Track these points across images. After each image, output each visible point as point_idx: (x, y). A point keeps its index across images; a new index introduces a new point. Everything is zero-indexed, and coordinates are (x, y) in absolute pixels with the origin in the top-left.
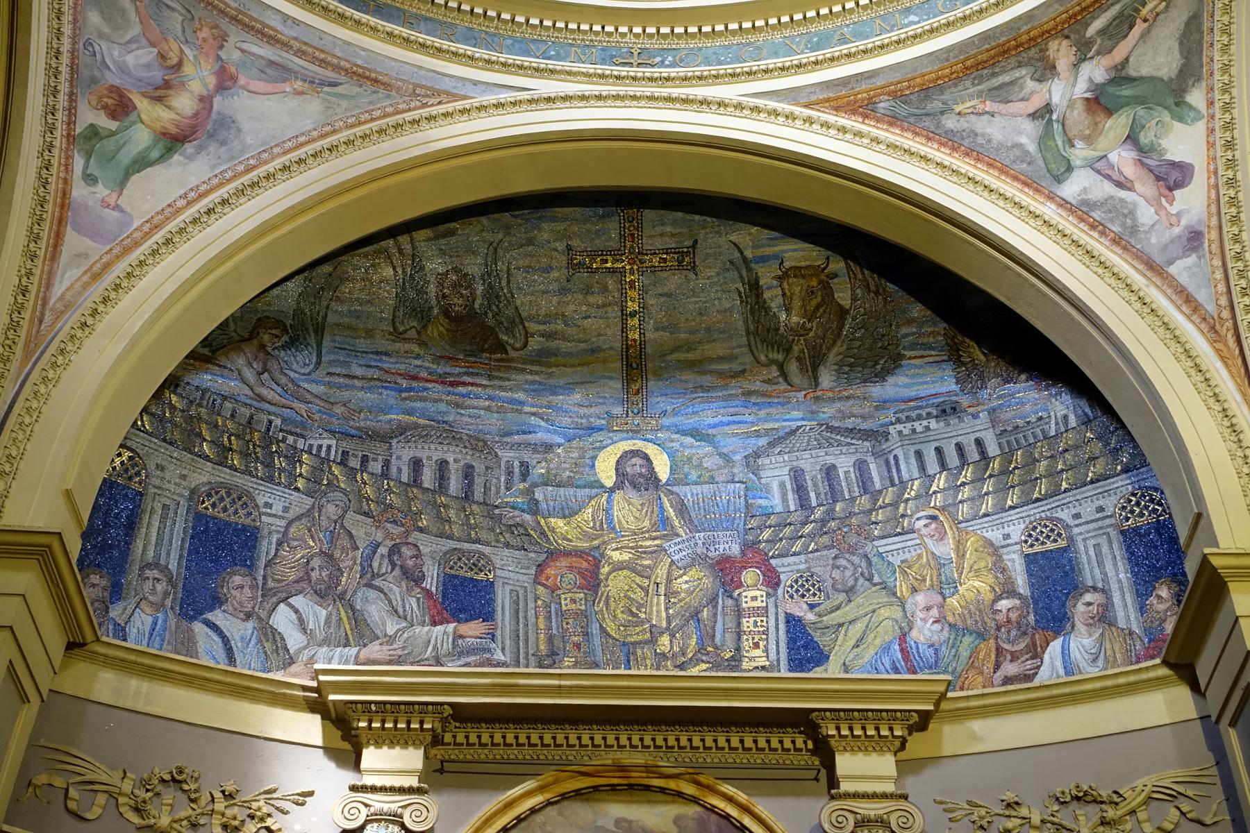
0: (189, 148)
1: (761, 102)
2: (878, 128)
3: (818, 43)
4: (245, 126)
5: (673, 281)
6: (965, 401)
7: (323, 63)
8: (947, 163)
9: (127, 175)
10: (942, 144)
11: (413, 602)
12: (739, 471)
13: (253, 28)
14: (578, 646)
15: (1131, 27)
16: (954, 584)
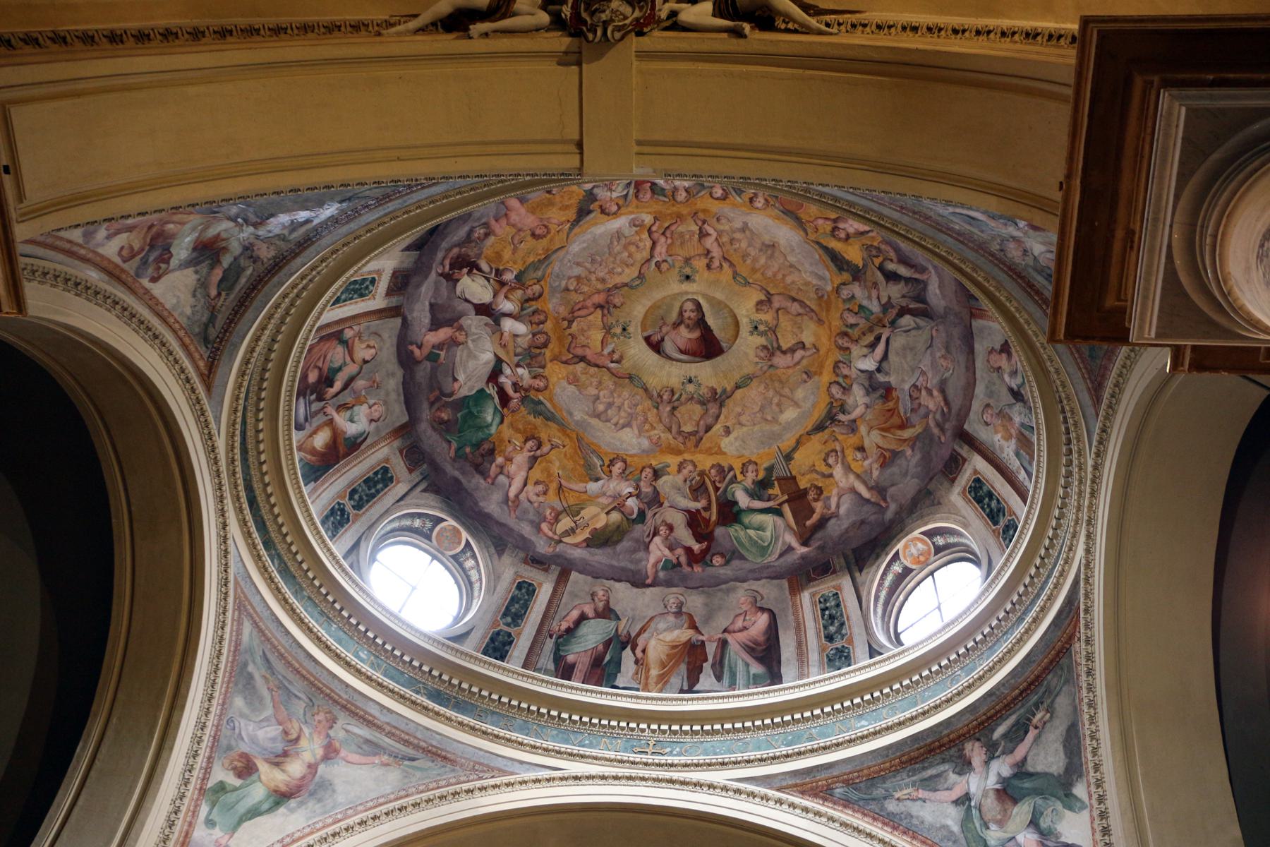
0: (293, 803)
1: (742, 786)
2: (834, 809)
3: (792, 740)
4: (339, 788)
7: (407, 743)
8: (887, 840)
9: (241, 821)
10: (885, 824)
13: (357, 714)
15: (1026, 732)
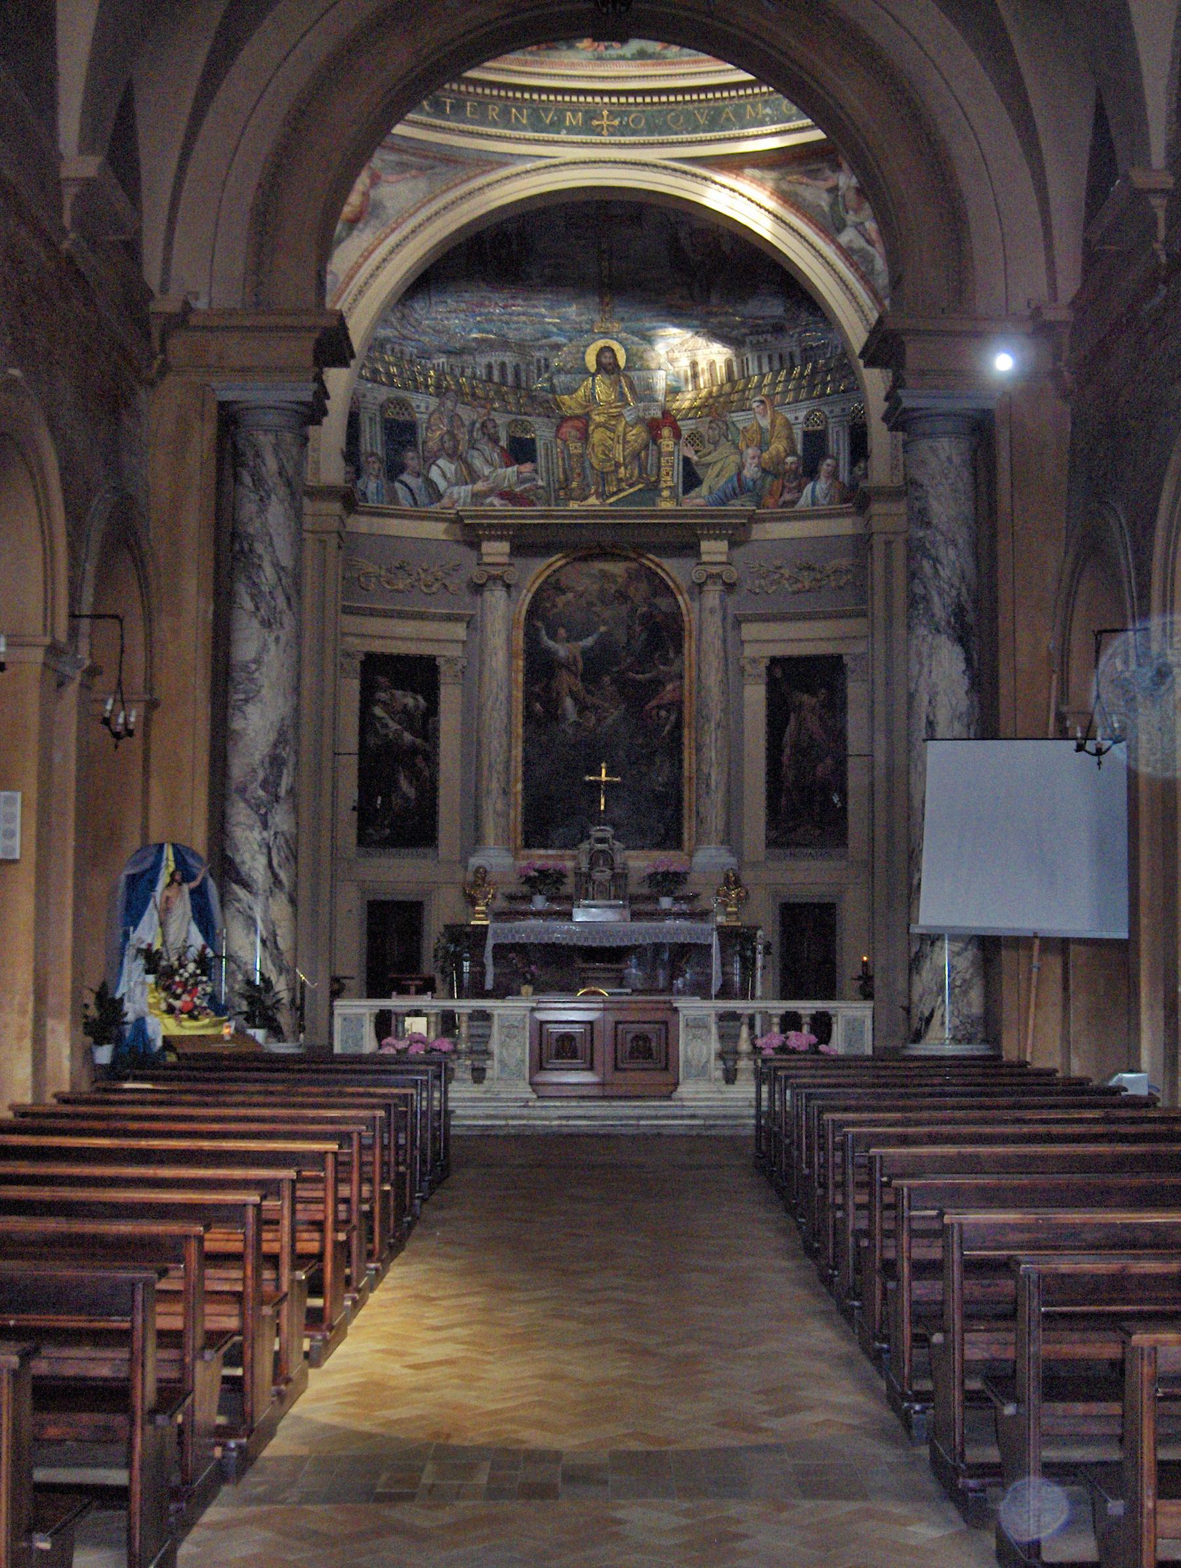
0: (360, 225)
4: (388, 204)
11: (496, 455)
14: (579, 475)
16: (768, 445)
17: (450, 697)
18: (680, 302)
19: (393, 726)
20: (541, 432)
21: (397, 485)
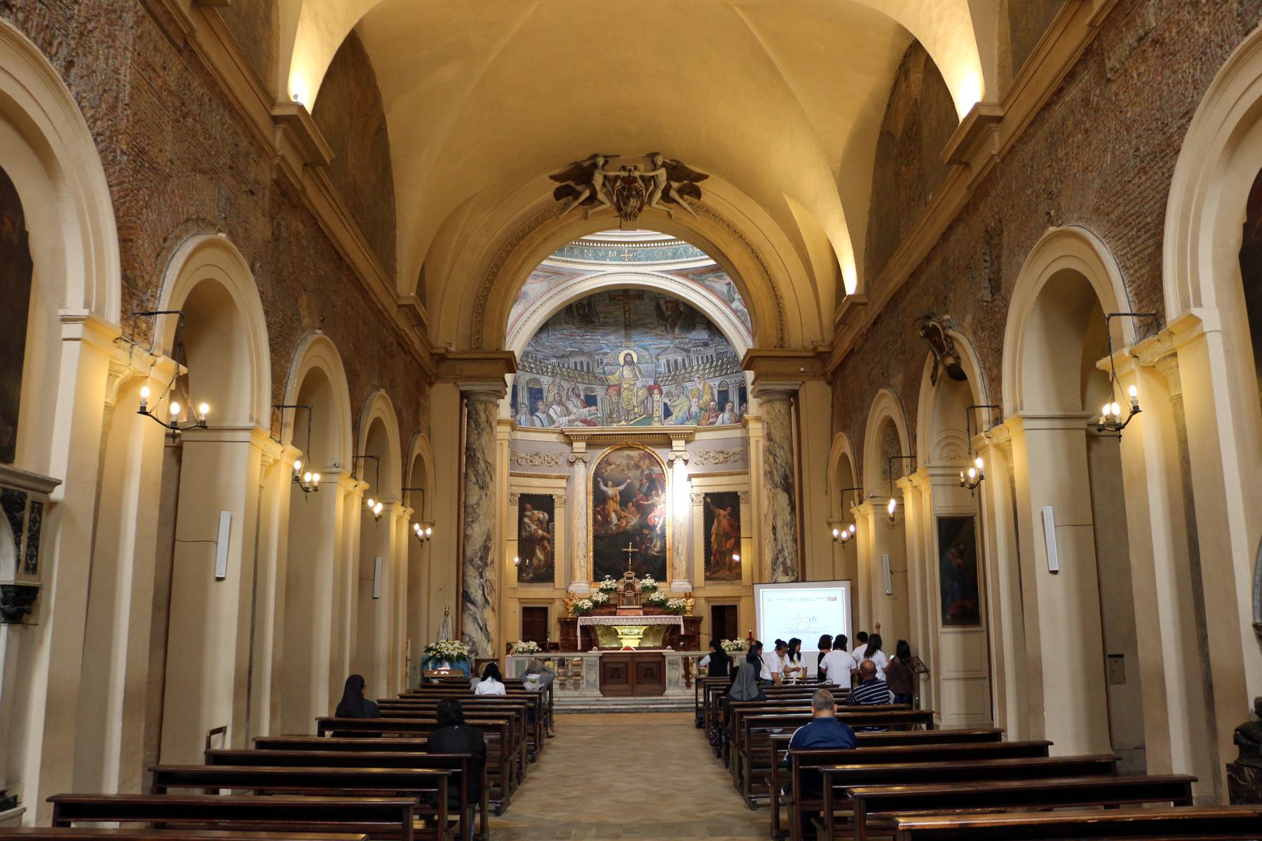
0: (518, 302)
5: (637, 302)
6: (710, 342)
12: (655, 361)
16: (702, 397)
17: (559, 513)
18: (661, 333)
19: (534, 527)
20: (599, 392)
21: (534, 417)
